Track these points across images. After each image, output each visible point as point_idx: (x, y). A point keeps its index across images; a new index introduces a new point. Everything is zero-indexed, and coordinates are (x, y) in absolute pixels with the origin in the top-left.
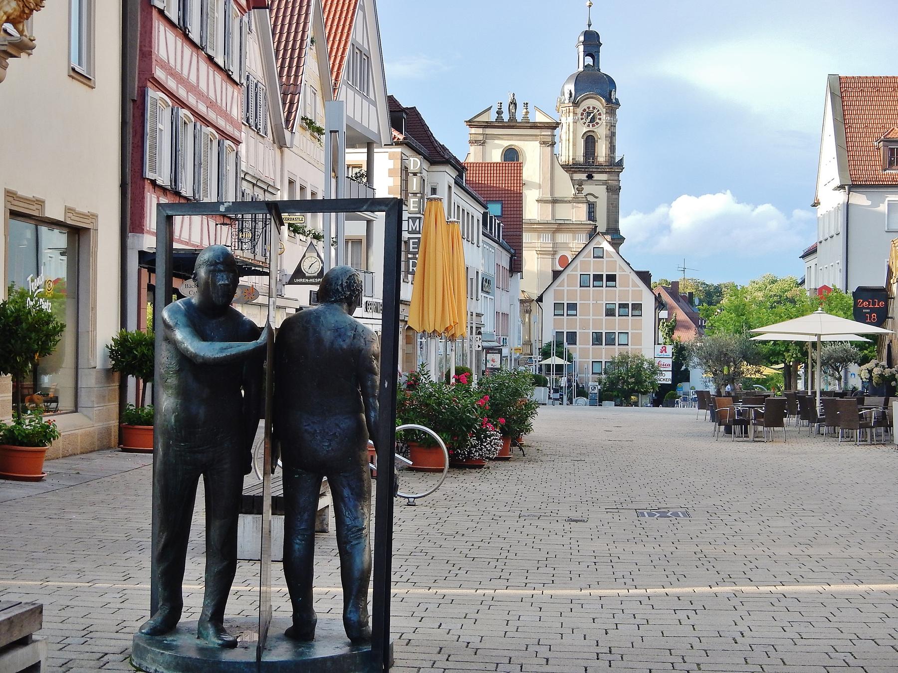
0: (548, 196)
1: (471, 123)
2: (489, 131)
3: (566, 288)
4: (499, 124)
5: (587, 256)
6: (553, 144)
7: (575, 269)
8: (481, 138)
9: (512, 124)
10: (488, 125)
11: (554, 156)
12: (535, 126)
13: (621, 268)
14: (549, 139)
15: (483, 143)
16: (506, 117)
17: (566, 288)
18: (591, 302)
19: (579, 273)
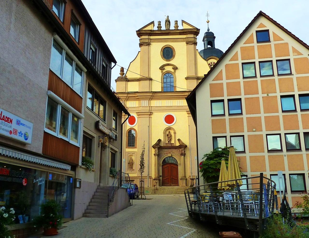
0: (193, 74)
1: (140, 33)
2: (152, 37)
3: (224, 81)
4: (160, 33)
5: (250, 41)
6: (195, 44)
7: (235, 58)
8: (147, 41)
9: (168, 32)
10: (151, 33)
11: (196, 50)
12: (183, 32)
13: (295, 50)
14: (193, 39)
15: (149, 44)
16: (163, 28)
17: (224, 81)
18: (260, 95)
19: (240, 62)
